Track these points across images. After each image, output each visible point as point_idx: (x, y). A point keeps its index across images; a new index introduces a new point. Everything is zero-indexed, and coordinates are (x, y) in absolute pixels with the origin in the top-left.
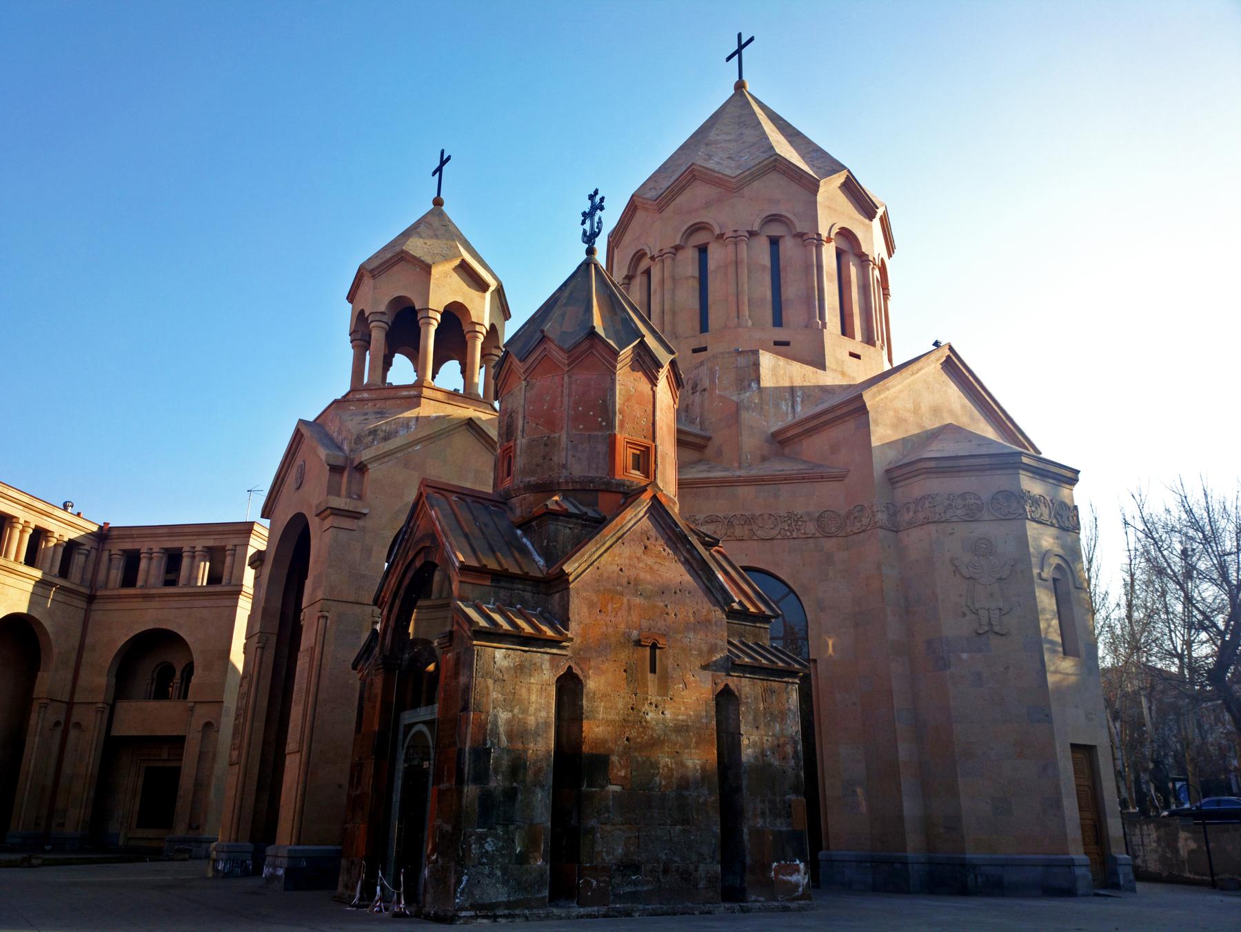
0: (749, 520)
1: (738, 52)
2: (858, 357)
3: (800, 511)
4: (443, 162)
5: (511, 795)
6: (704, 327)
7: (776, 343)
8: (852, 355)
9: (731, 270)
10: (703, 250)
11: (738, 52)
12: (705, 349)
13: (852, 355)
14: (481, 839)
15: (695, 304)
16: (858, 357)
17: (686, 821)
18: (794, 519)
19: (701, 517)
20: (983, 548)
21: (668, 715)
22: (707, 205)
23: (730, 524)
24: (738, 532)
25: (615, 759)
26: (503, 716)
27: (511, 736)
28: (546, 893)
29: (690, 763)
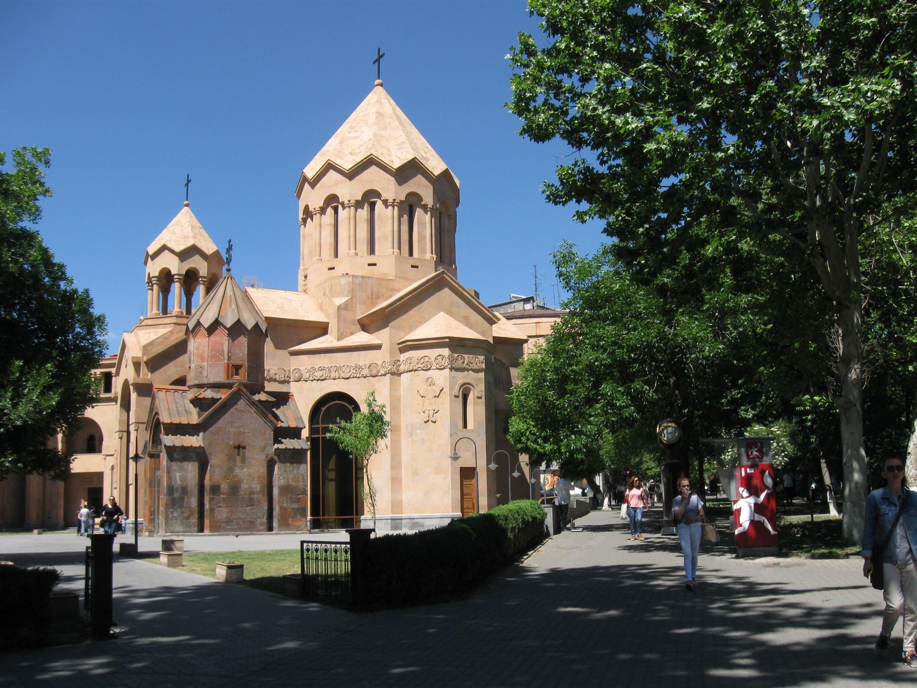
0: (338, 369)
1: (378, 60)
2: (417, 267)
3: (361, 364)
4: (189, 181)
5: (182, 499)
6: (336, 256)
7: (369, 265)
8: (413, 267)
9: (347, 222)
10: (336, 210)
11: (378, 60)
12: (333, 268)
13: (413, 267)
14: (172, 512)
15: (331, 240)
16: (417, 267)
17: (253, 505)
18: (358, 368)
19: (316, 367)
20: (431, 382)
21: (245, 470)
22: (336, 184)
23: (330, 371)
24: (333, 375)
25: (222, 486)
26: (178, 475)
27: (181, 480)
28: (196, 528)
29: (254, 486)
